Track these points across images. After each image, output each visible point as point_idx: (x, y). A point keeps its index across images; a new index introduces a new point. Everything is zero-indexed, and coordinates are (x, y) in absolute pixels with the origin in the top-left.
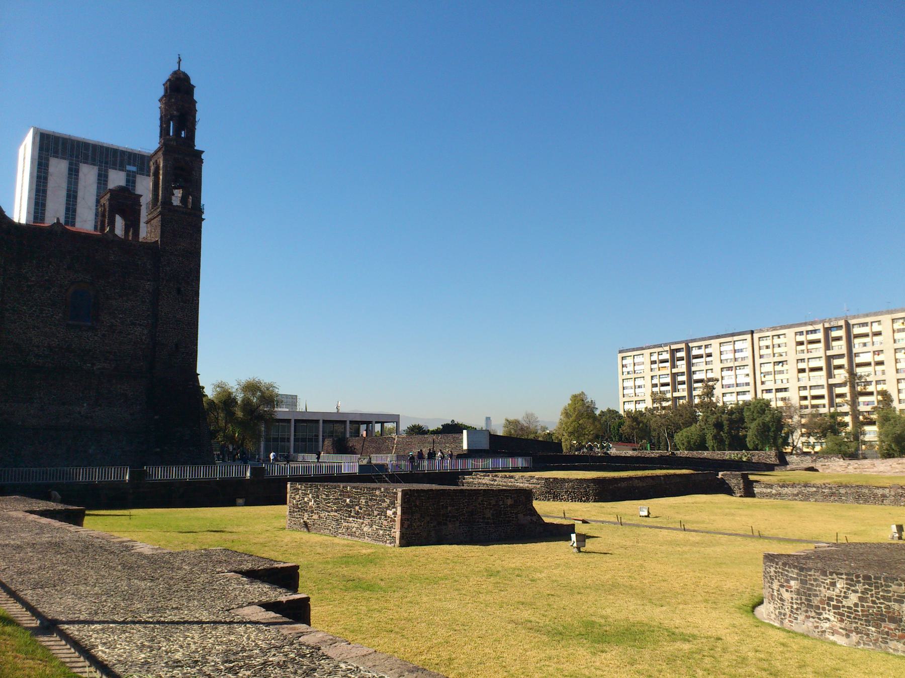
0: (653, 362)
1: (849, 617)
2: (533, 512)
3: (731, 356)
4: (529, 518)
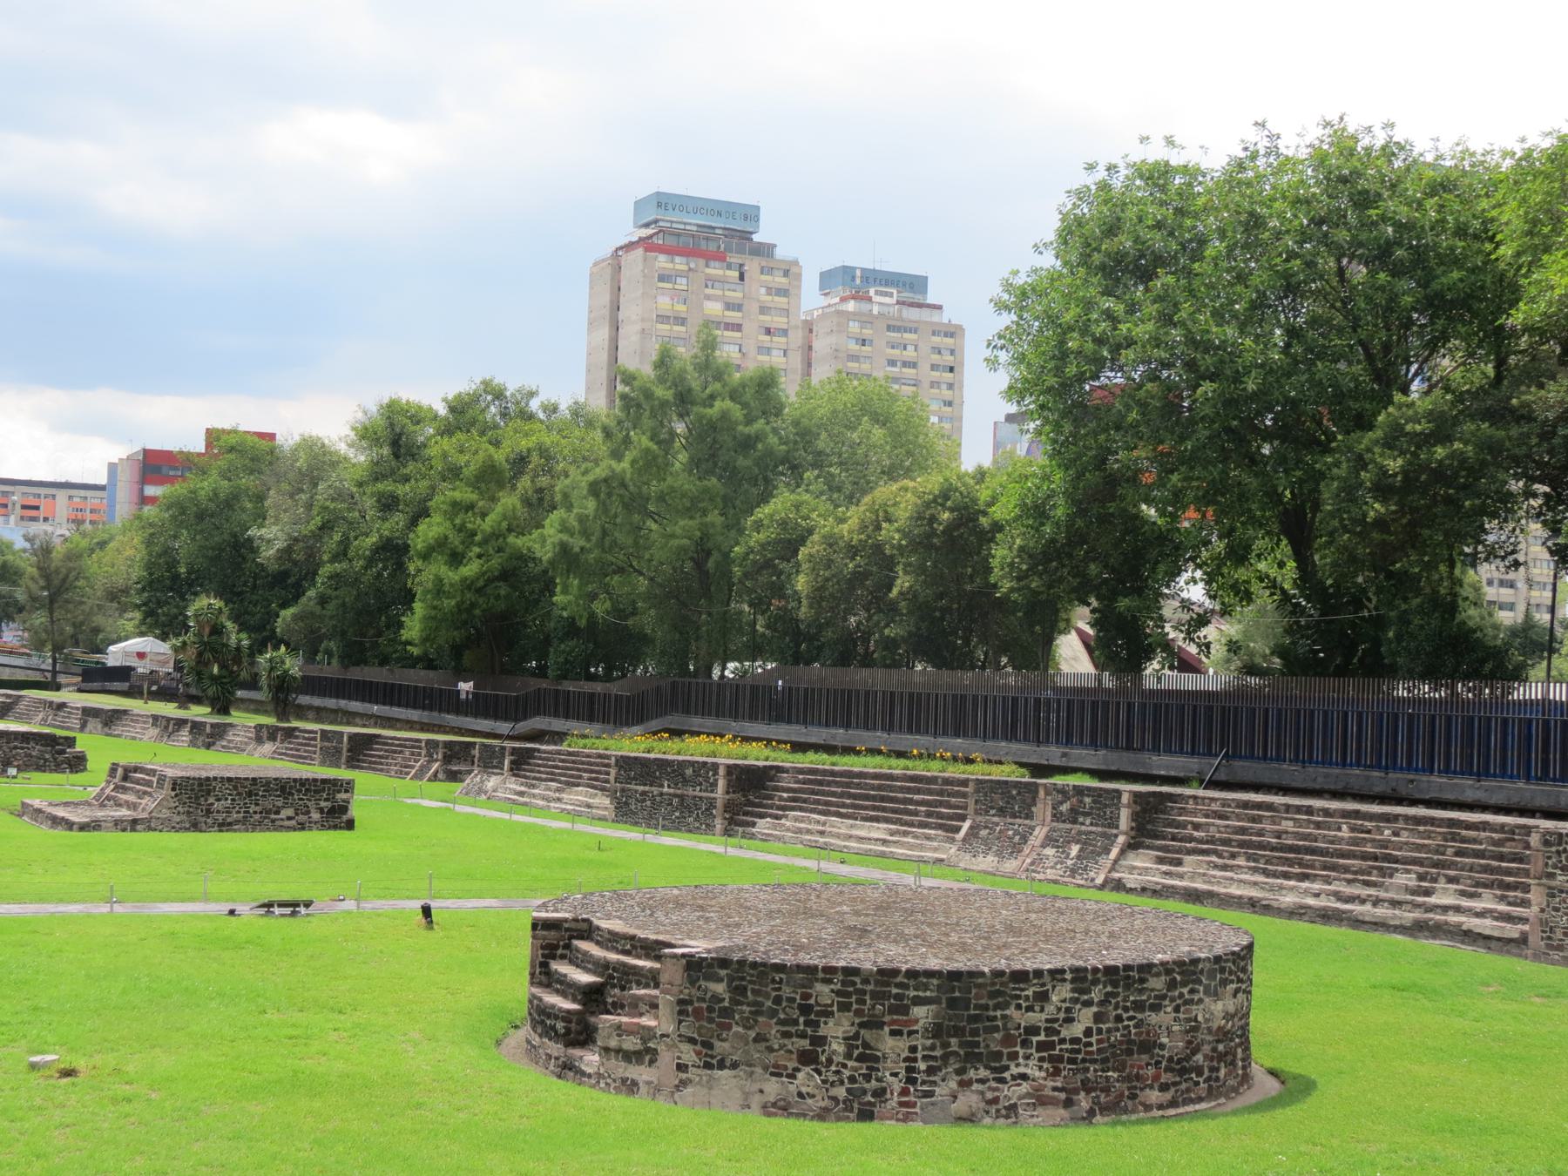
1: (1072, 1061)
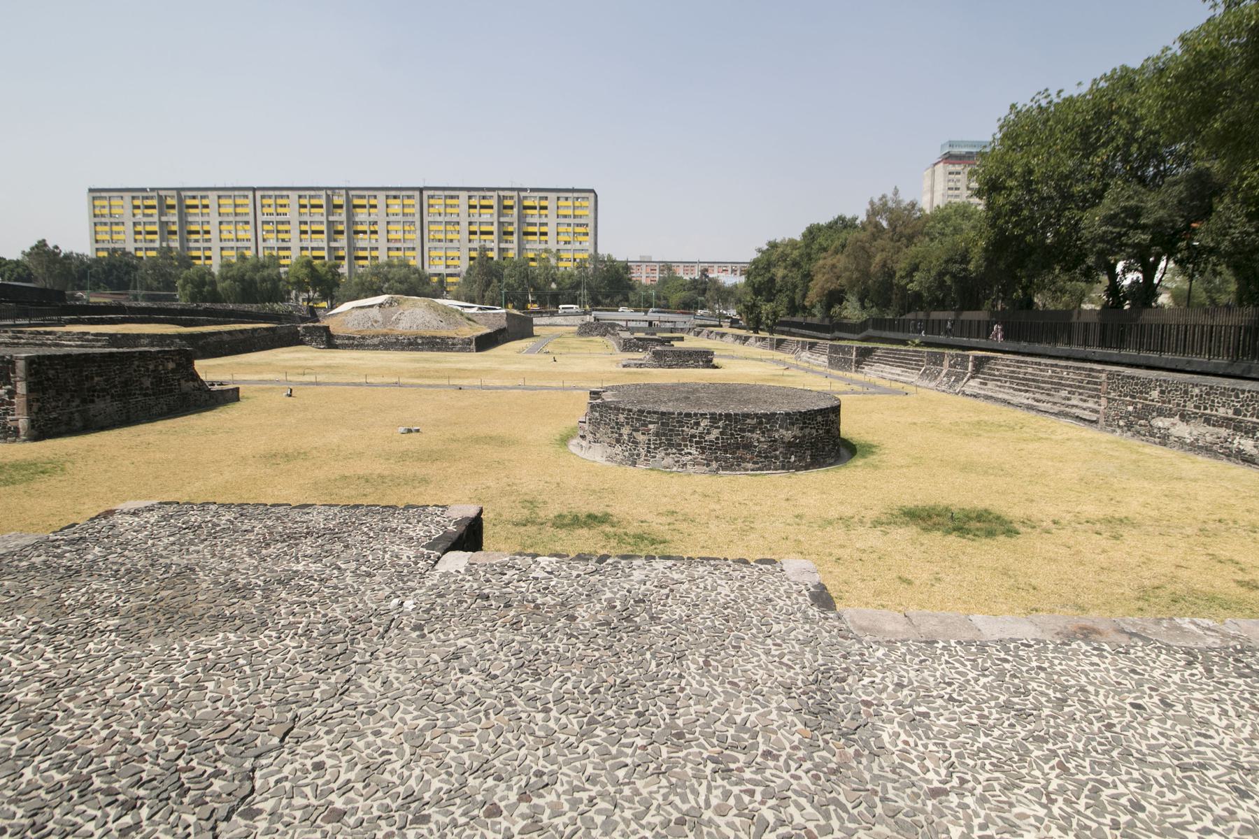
2: (195, 377)
3: (231, 210)
4: (191, 384)
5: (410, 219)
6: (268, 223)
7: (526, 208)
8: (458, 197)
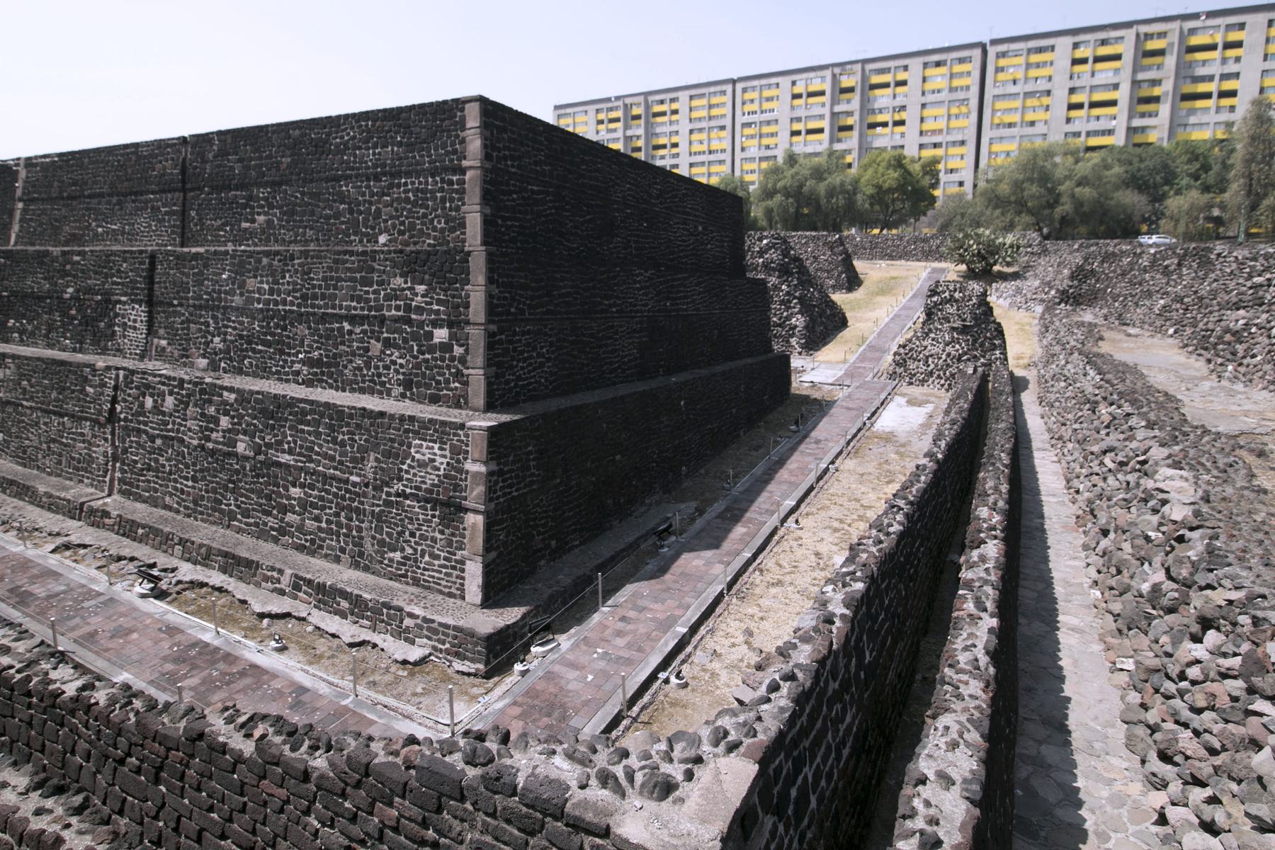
0: (600, 122)
5: (961, 95)
6: (748, 125)
7: (1193, 49)
8: (1053, 48)
